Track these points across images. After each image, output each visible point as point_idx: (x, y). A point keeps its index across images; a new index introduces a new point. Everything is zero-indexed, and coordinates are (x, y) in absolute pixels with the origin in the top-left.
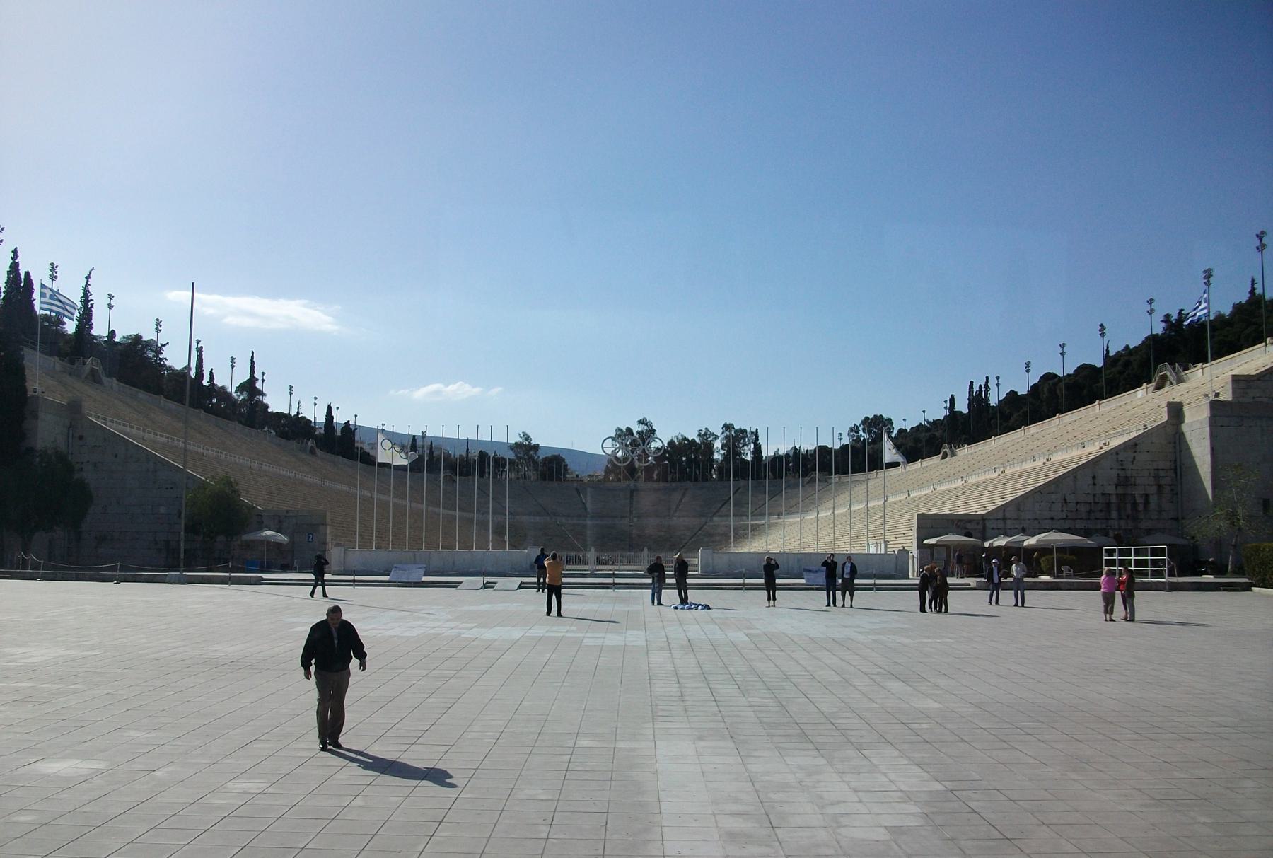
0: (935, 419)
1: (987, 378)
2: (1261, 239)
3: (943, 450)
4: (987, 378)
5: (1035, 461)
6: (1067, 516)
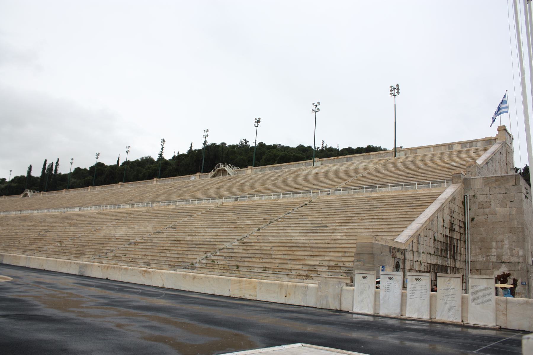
0: (181, 153)
1: (58, 159)
2: (316, 106)
3: (24, 193)
4: (58, 159)
5: (236, 200)
6: (434, 252)
